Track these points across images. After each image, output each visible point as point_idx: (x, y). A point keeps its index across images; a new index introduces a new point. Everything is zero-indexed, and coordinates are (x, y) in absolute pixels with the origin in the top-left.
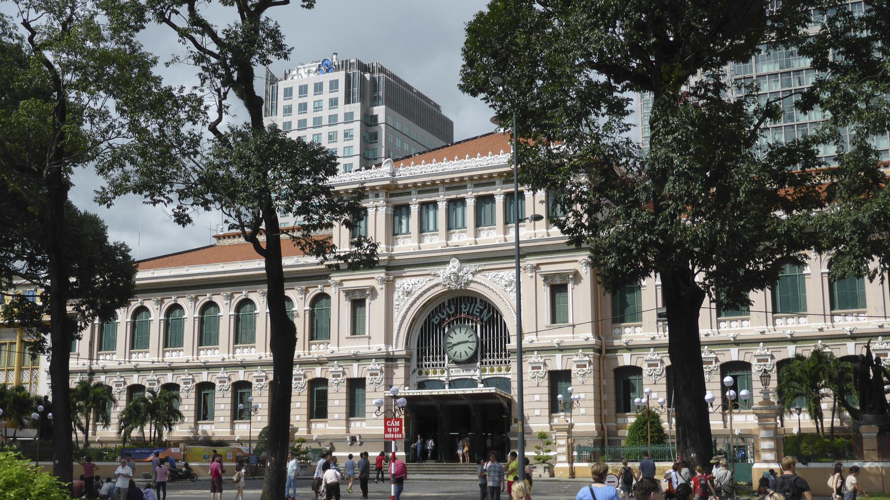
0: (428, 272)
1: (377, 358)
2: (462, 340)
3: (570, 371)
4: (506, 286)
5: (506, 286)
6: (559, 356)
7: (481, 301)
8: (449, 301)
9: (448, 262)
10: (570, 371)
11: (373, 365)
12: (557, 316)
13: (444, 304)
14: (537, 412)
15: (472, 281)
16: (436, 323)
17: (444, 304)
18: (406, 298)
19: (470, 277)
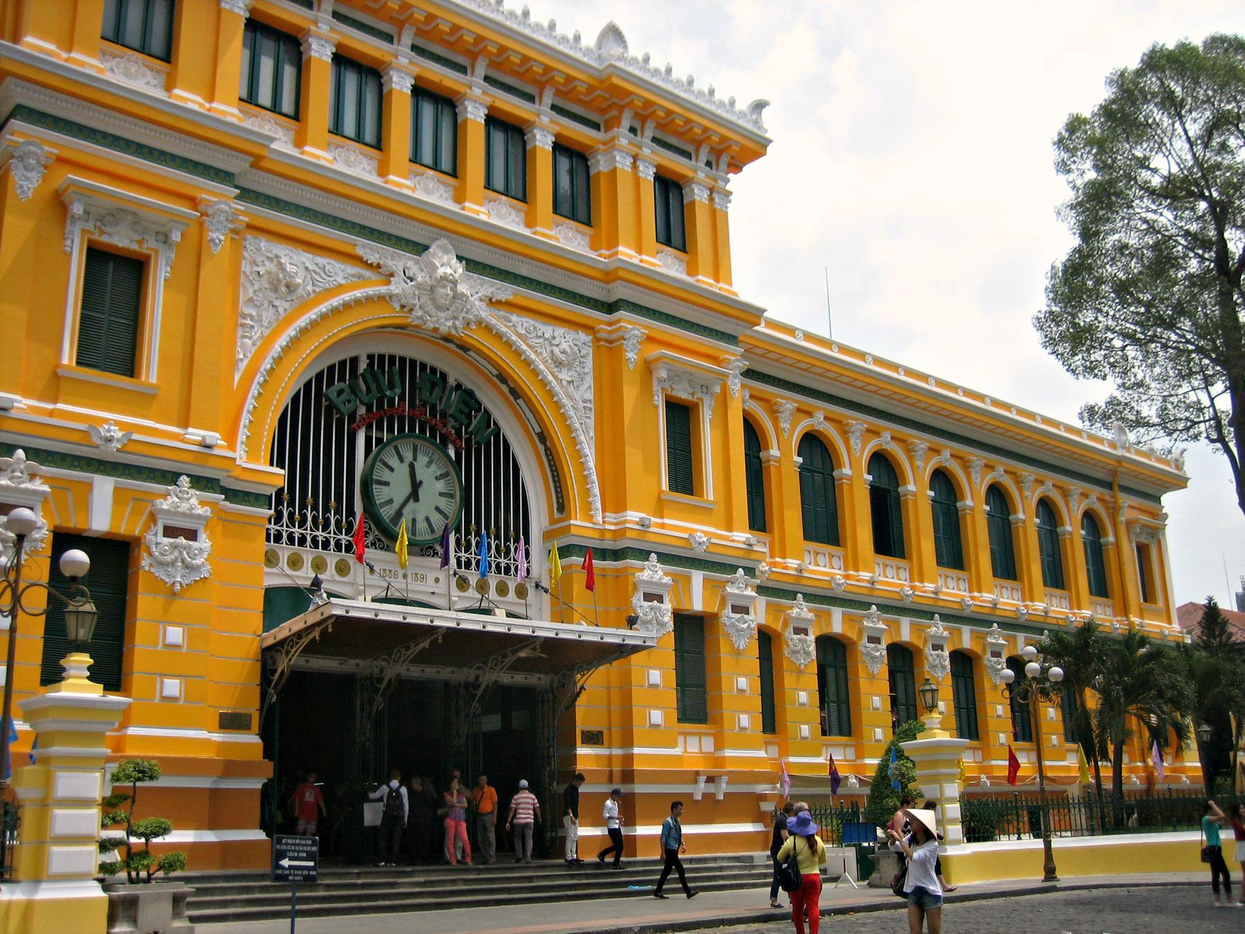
0: (360, 251)
1: (200, 482)
2: (415, 481)
3: (715, 616)
4: (559, 364)
5: (559, 364)
6: (697, 577)
7: (459, 386)
8: (371, 357)
9: (426, 248)
10: (715, 616)
11: (185, 501)
12: (684, 475)
13: (355, 361)
14: (657, 716)
15: (479, 322)
16: (346, 409)
17: (355, 361)
18: (287, 305)
19: (485, 313)
